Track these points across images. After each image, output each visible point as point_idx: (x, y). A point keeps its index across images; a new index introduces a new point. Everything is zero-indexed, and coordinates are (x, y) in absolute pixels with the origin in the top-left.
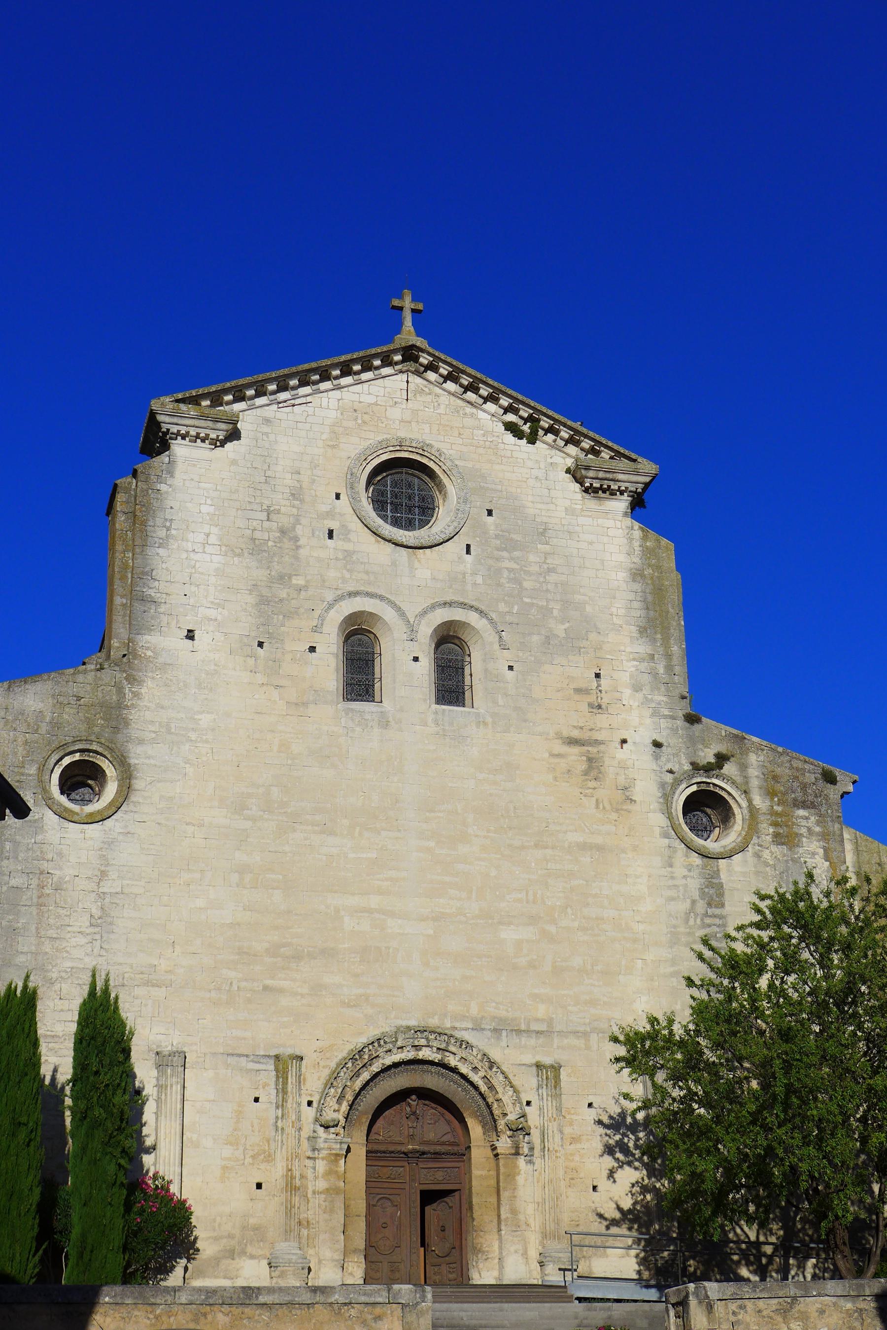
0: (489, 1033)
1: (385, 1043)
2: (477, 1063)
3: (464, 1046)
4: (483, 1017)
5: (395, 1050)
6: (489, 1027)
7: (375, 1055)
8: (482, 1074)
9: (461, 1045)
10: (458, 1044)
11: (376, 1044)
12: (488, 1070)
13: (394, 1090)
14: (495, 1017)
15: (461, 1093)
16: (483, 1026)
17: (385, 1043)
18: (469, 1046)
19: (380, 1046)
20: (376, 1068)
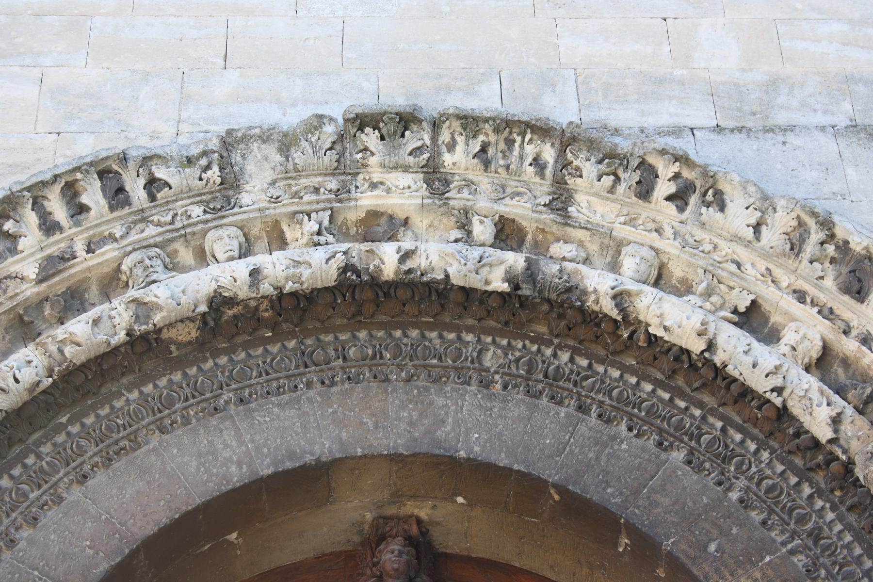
0: (828, 145)
1: (153, 185)
2: (752, 284)
3: (664, 188)
4: (773, 84)
5: (222, 241)
6: (822, 119)
7: (84, 263)
8: (804, 331)
9: (644, 191)
10: (629, 178)
11: (93, 195)
12: (845, 306)
13: (236, 476)
14: (849, 80)
15: (690, 479)
16: (781, 118)
17: (153, 185)
18: (697, 190)
19: (117, 196)
20: (82, 334)
